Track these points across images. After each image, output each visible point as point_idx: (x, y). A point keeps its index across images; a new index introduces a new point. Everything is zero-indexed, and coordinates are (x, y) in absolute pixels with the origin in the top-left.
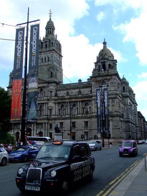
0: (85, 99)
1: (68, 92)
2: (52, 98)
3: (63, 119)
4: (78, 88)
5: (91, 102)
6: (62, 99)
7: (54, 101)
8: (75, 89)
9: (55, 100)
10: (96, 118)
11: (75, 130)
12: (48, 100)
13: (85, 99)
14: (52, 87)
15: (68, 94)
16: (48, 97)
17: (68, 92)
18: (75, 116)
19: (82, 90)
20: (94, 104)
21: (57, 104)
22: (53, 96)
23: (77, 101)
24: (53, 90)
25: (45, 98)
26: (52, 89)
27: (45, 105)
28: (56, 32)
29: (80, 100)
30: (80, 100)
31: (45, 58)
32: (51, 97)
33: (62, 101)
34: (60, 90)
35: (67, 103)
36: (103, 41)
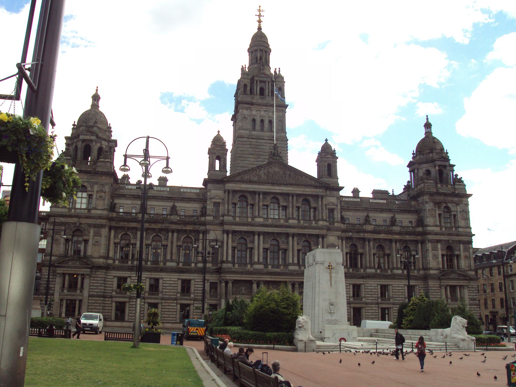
0: (408, 237)
1: (367, 216)
2: (336, 224)
3: (363, 277)
4: (390, 211)
5: (420, 245)
6: (358, 232)
7: (339, 233)
8: (382, 211)
9: (344, 231)
10: (406, 279)
11: (388, 304)
12: (329, 229)
13: (408, 237)
14: (334, 200)
15: (367, 221)
16: (326, 221)
17: (367, 216)
18: (387, 272)
19: (399, 217)
20: (433, 250)
21: (344, 242)
22: (337, 222)
23: (391, 241)
24: (337, 206)
25: (321, 223)
26: (334, 204)
27: (320, 239)
28: (275, 63)
29: (397, 237)
30: (397, 237)
31: (262, 121)
32: (332, 222)
33: (355, 235)
34: (348, 210)
35: (369, 240)
36: (425, 121)
